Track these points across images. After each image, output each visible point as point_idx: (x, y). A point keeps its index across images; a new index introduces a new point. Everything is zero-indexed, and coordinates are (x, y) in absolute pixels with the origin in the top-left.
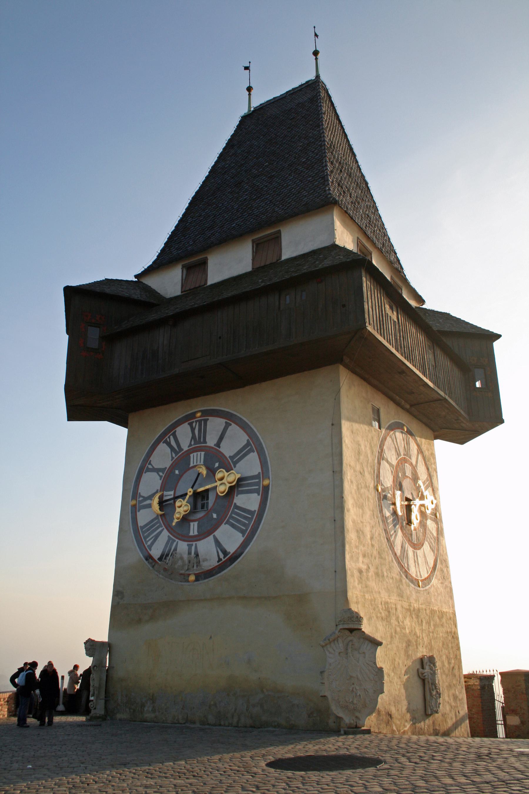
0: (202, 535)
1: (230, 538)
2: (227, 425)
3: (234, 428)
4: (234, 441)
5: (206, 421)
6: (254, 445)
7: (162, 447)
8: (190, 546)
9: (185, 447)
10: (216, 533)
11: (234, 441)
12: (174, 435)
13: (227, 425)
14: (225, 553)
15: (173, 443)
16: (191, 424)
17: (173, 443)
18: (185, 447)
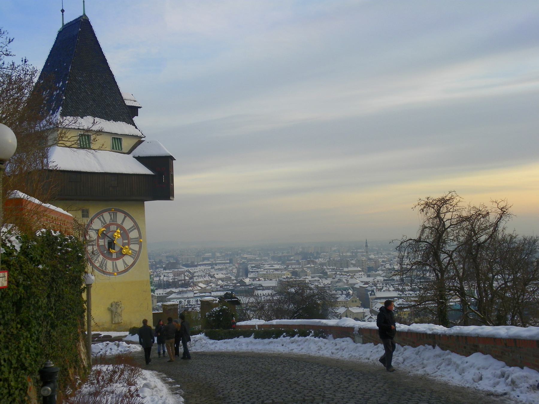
0: (117, 259)
1: (129, 260)
2: (125, 217)
3: (127, 218)
4: (128, 224)
5: (116, 213)
6: (136, 226)
7: (96, 220)
8: (113, 262)
9: (108, 222)
10: (124, 258)
11: (128, 224)
12: (102, 216)
13: (125, 217)
14: (127, 266)
15: (102, 219)
16: (109, 213)
17: (102, 219)
18: (108, 222)
